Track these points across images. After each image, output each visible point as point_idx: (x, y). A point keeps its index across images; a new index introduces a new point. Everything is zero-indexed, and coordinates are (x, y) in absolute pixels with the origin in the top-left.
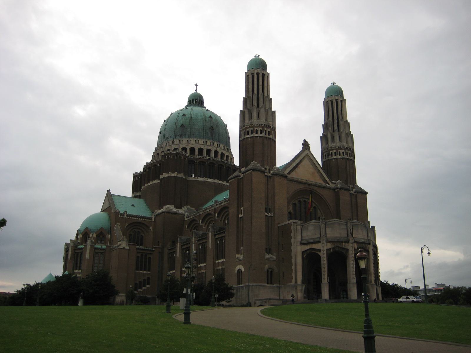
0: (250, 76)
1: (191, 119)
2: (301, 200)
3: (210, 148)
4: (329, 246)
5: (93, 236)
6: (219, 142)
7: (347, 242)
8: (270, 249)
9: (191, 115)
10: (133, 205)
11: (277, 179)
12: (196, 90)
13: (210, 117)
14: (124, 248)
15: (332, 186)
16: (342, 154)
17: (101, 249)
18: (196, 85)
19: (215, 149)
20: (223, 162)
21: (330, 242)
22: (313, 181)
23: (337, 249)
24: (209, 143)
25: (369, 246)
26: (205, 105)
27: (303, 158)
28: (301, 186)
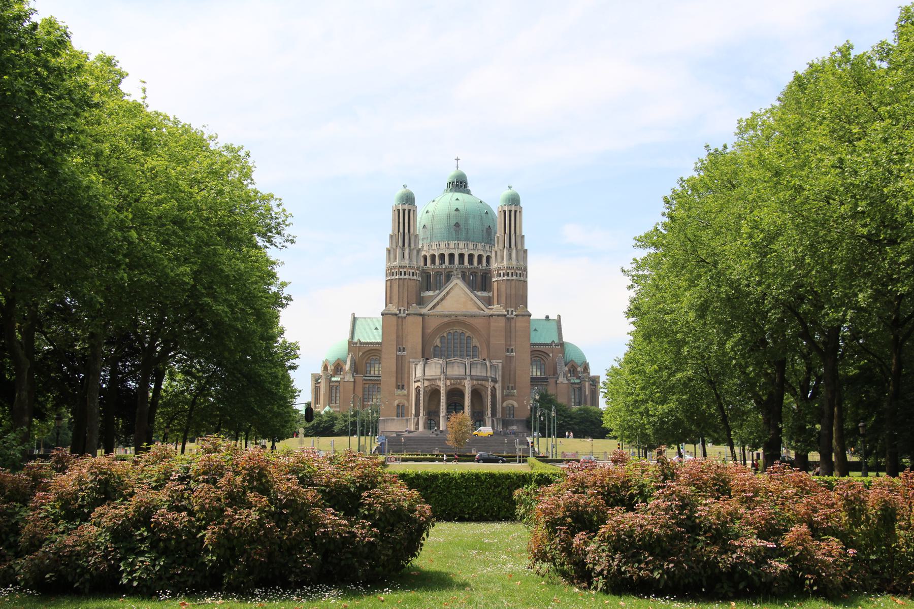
0: (397, 212)
1: (433, 216)
2: (451, 331)
3: (452, 251)
4: (426, 384)
5: (330, 368)
6: (468, 240)
7: (440, 379)
8: (403, 386)
9: (434, 211)
10: (376, 329)
11: (409, 319)
12: (457, 167)
13: (457, 210)
14: (348, 381)
15: (487, 312)
16: (502, 275)
17: (336, 382)
18: (458, 159)
19: (460, 252)
20: (466, 268)
21: (428, 380)
22: (464, 310)
23: (433, 386)
24: (452, 246)
25: (466, 381)
26: (470, 187)
27: (452, 288)
28: (446, 319)
